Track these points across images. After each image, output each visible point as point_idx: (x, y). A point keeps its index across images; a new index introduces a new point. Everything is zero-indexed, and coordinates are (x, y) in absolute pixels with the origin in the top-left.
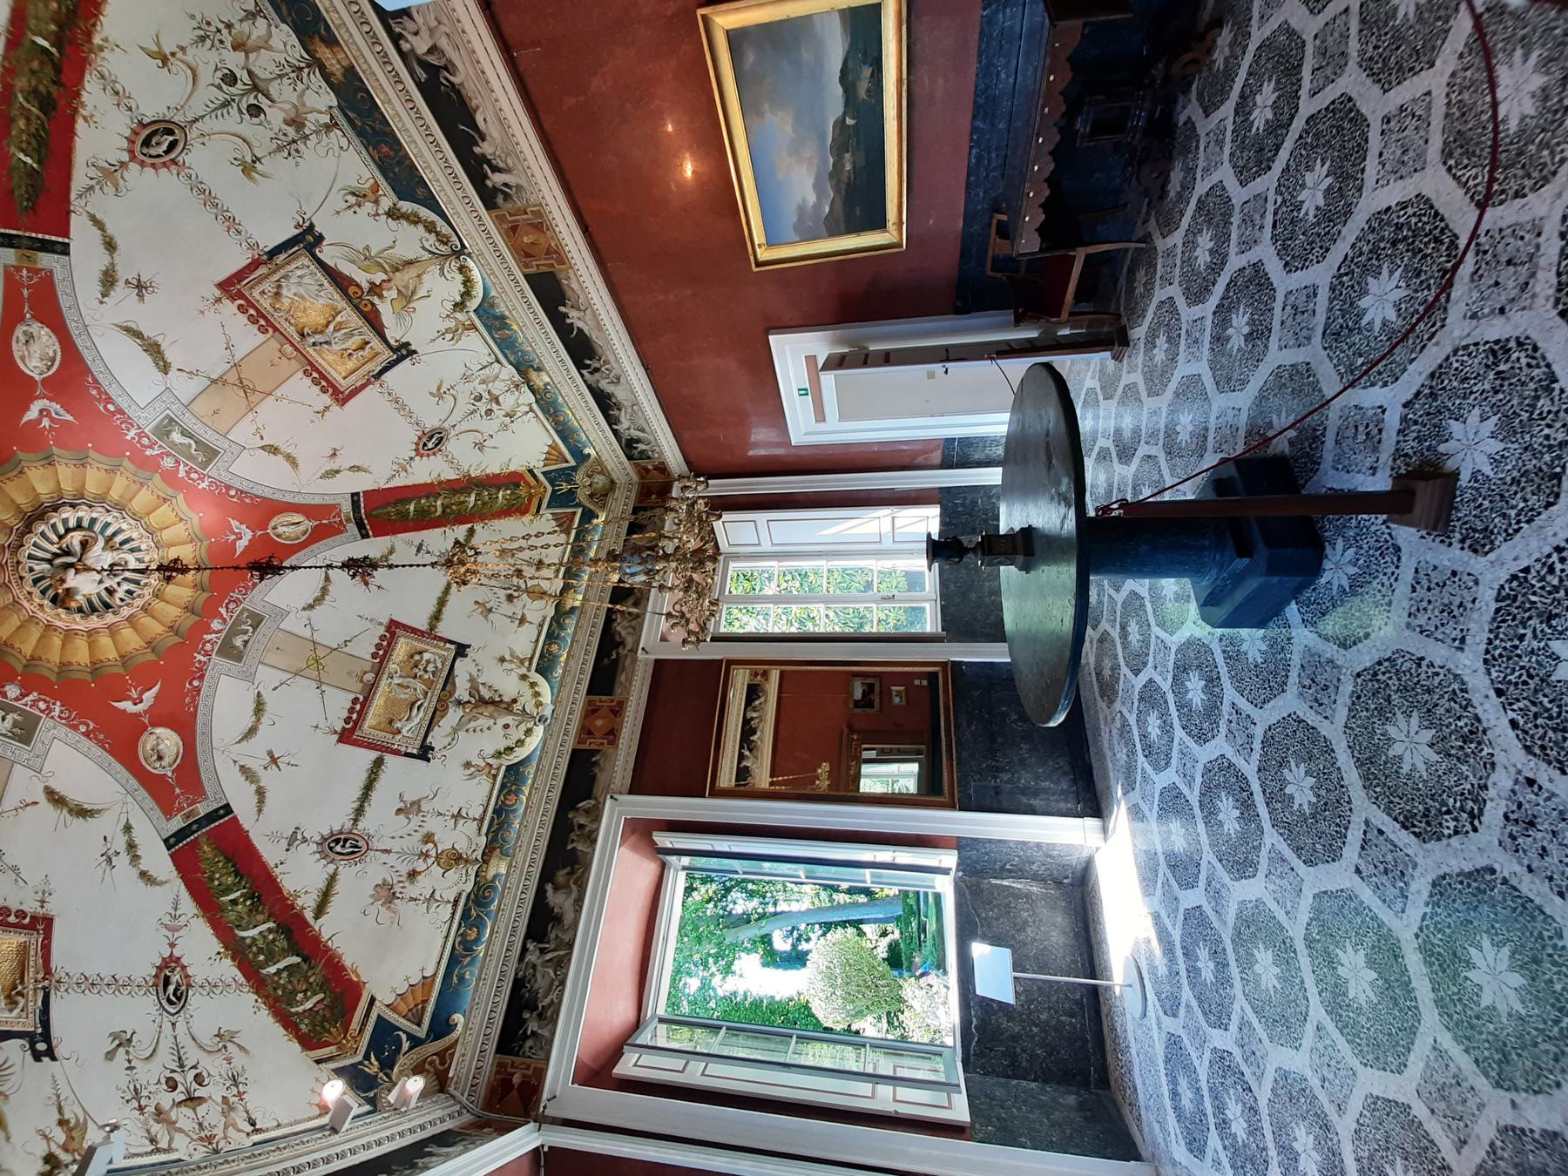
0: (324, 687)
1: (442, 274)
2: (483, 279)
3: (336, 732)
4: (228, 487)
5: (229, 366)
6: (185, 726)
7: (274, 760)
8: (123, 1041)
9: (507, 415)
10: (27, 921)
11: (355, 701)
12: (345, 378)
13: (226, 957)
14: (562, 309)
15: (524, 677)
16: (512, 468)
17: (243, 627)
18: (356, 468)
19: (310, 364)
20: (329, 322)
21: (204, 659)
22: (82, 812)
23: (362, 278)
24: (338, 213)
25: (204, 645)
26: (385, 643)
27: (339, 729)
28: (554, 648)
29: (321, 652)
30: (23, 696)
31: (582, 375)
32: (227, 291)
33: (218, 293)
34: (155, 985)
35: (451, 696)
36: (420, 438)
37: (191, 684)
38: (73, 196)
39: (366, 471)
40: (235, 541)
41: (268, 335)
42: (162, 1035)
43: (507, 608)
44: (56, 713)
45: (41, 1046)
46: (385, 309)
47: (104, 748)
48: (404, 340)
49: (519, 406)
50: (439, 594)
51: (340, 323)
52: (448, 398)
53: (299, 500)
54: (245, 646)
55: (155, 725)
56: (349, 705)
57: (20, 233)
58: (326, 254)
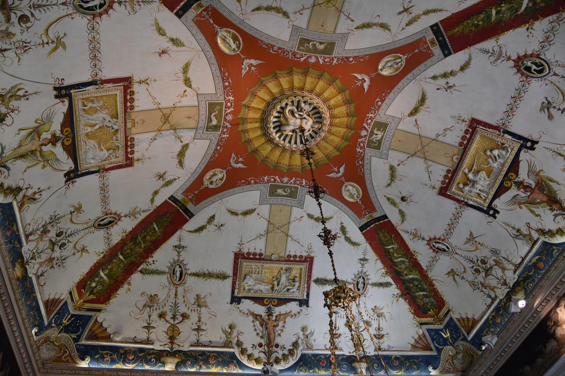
4: (225, 87)
5: (162, 132)
6: (376, 57)
7: (406, 10)
8: (547, 106)
10: (470, 130)
12: (116, 95)
13: (533, 24)
17: (311, 46)
19: (125, 111)
21: (336, 60)
22: (423, 100)
23: (59, 151)
24: (49, 188)
25: (327, 62)
30: (365, 129)
33: (136, 163)
34: (527, 77)
36: (100, 15)
37: (352, 61)
38: (152, 211)
39: (157, 24)
40: (254, 66)
41: (132, 136)
42: (557, 84)
44: (373, 115)
45: (529, 144)
46: (56, 127)
47: (389, 93)
48: (58, 100)
51: (90, 126)
53: (208, 47)
54: (323, 43)
57: (179, 208)
58: (68, 165)
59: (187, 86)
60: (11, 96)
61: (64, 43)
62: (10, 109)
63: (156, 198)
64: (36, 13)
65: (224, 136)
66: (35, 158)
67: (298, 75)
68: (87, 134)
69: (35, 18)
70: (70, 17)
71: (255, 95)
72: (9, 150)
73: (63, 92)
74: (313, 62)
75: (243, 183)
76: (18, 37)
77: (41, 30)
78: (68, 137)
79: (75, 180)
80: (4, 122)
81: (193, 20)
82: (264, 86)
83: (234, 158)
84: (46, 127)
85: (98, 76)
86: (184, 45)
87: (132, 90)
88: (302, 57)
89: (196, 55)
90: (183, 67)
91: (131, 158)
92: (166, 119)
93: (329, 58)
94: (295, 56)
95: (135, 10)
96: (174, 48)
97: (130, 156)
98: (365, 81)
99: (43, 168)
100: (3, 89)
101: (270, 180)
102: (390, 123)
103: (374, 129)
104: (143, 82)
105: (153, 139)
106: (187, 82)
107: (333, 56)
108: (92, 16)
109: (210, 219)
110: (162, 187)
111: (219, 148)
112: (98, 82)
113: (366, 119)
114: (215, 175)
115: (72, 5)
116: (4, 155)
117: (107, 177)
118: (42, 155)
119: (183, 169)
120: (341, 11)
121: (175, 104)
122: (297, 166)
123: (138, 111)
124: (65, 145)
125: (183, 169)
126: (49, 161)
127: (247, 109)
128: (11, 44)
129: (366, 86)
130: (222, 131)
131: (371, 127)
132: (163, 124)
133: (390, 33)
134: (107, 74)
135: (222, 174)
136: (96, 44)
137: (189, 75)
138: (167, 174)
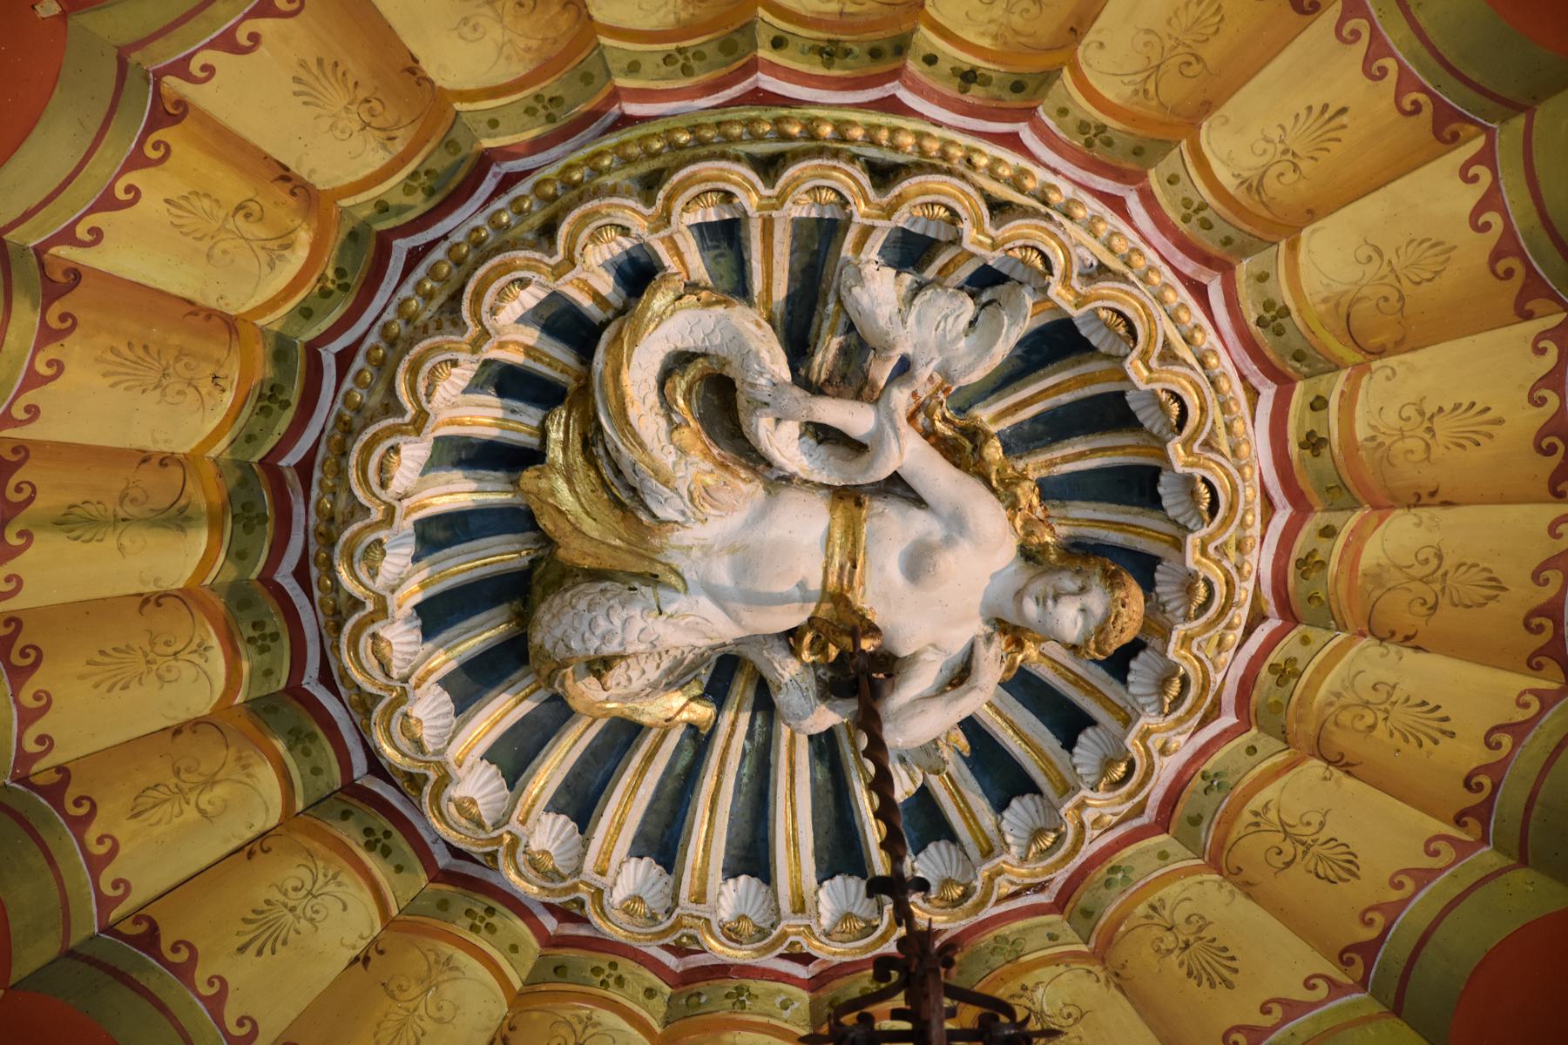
71: (167, 114)
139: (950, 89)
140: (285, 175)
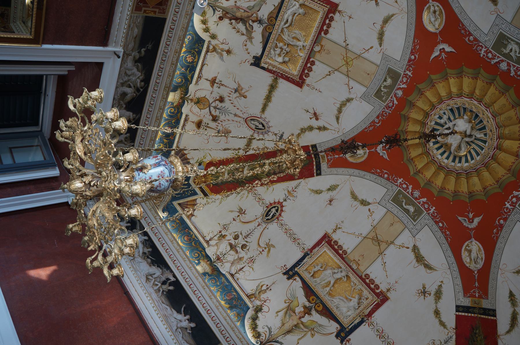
0: (344, 44)
1: (270, 329)
2: (245, 332)
3: (339, 12)
4: (388, 179)
5: (385, 253)
9: (224, 236)
11: (326, 32)
12: (325, 251)
14: (193, 325)
15: (213, 37)
16: (218, 196)
17: (386, 90)
18: (318, 192)
19: (343, 258)
20: (333, 286)
21: (407, 72)
23: (316, 317)
25: (407, 81)
26: (306, 71)
27: (337, 14)
28: (189, 60)
29: (344, 69)
30: (499, 63)
31: (174, 276)
32: (384, 296)
33: (389, 295)
35: (266, 27)
36: (280, 215)
37: (415, 57)
38: (454, 337)
41: (365, 273)
43: (224, 92)
44: (484, 50)
46: (302, 300)
47: (463, 25)
48: (291, 281)
49: (216, 244)
50: (270, 104)
51: (327, 286)
52: (262, 245)
53: (351, 171)
54: (386, 78)
55: (435, 34)
56: (330, 30)
57: (479, 316)
58: (334, 327)
59: (367, 205)
60: (259, 292)
61: (272, 244)
62: (263, 301)
63: (443, 319)
64: (248, 239)
65: (431, 211)
66: (301, 330)
67: (410, 112)
68: (329, 294)
69: (249, 242)
70: (266, 229)
71: (412, 159)
72: (276, 329)
73: (291, 273)
74: (402, 93)
75: (497, 233)
76: (246, 257)
77: (256, 246)
78: (317, 304)
79: (349, 337)
80: (262, 311)
81: (328, 168)
82: (407, 147)
83: (466, 220)
84: (295, 303)
85: (305, 249)
86: (338, 185)
87: (333, 240)
88: (393, 101)
89: (350, 182)
90: (351, 197)
91: (380, 292)
92: (377, 240)
93: (403, 77)
94: (389, 107)
95: (295, 196)
96: (335, 192)
97: (378, 291)
98: (443, 49)
99: (313, 337)
100: (252, 290)
101: (512, 203)
102: (501, 30)
103: (503, 51)
104: (336, 230)
105: (383, 264)
106: (364, 203)
107: (403, 73)
108: (277, 219)
109: (511, 300)
110: (436, 303)
111: (441, 225)
112: (308, 252)
113: (487, 59)
114: (470, 252)
115: (263, 223)
116: (272, 333)
117: (375, 322)
118: (306, 327)
119: (436, 270)
120: (359, 56)
121: (373, 225)
122: (514, 163)
123: (352, 251)
124: (319, 311)
125: (436, 270)
126: (315, 329)
127: (420, 175)
128: (244, 263)
129: (448, 49)
130: (425, 209)
131: (498, 55)
132: (380, 246)
133: (396, 15)
134: (310, 244)
135: (474, 243)
136: (289, 232)
137: (360, 198)
138: (427, 287)
139: (431, 111)
140: (419, 155)
